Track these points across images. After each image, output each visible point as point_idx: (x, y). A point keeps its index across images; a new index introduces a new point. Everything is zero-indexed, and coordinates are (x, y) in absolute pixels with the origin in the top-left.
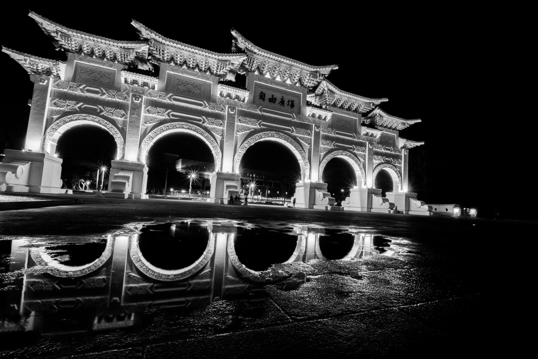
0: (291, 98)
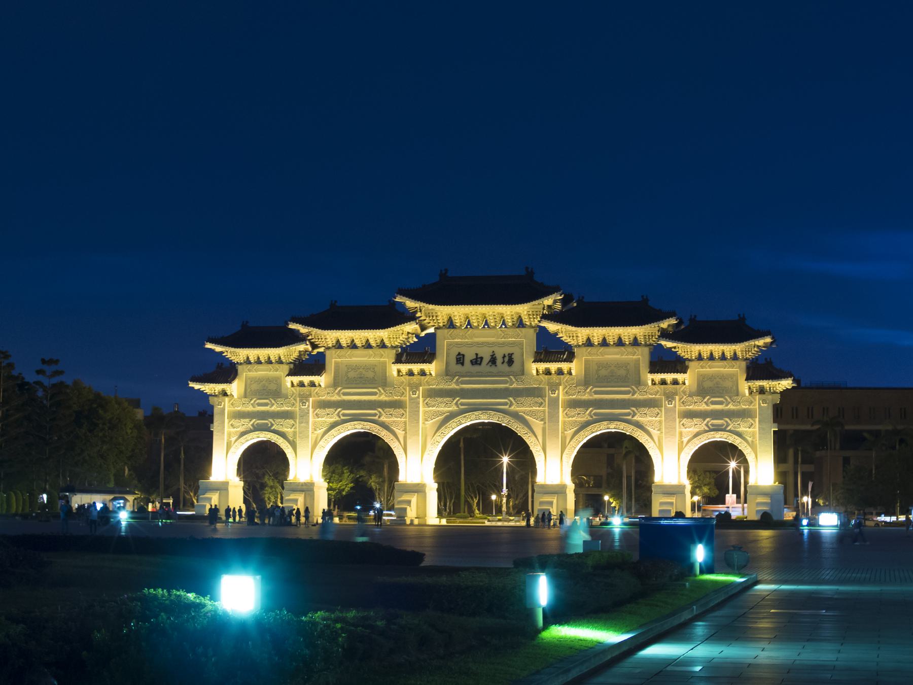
0: (507, 350)
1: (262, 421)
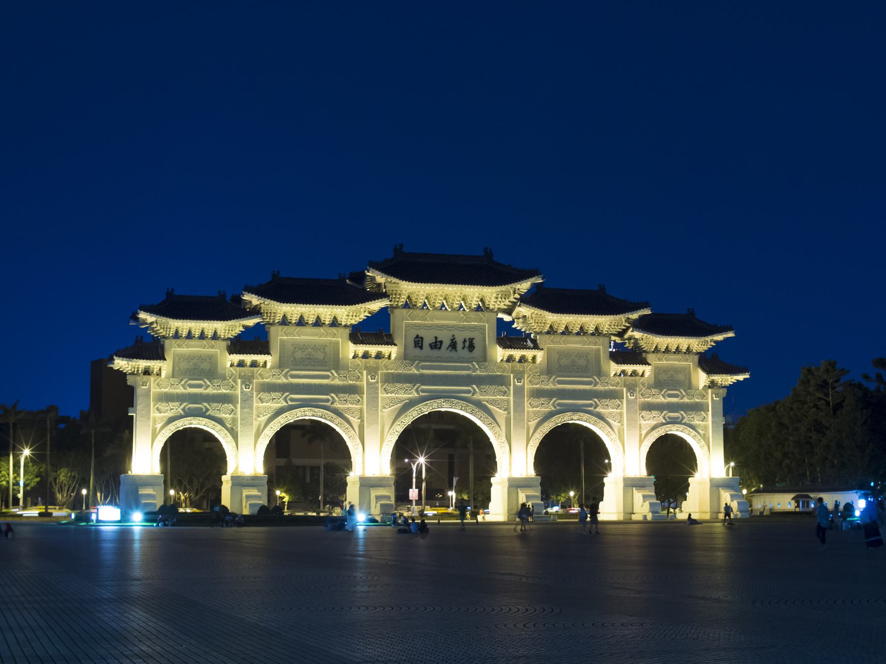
0: (468, 335)
1: (196, 405)
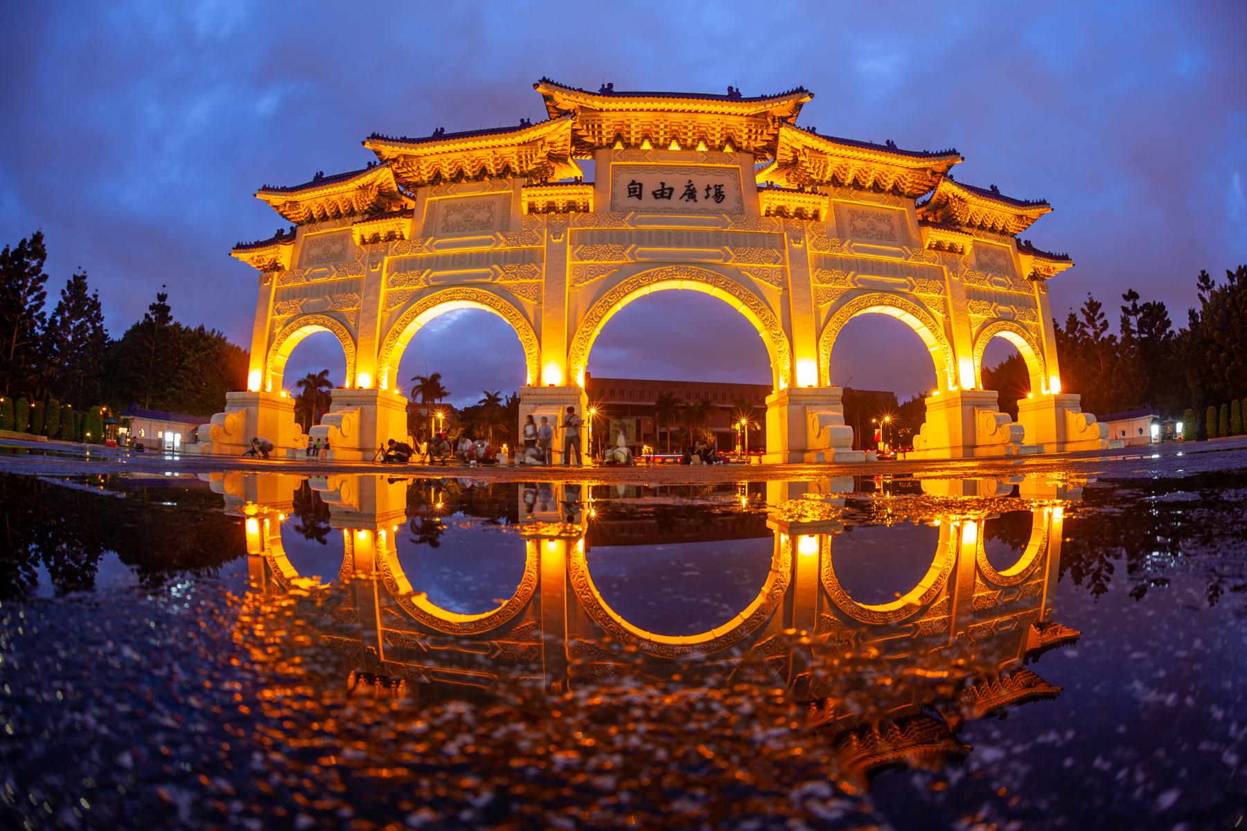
0: (713, 180)
